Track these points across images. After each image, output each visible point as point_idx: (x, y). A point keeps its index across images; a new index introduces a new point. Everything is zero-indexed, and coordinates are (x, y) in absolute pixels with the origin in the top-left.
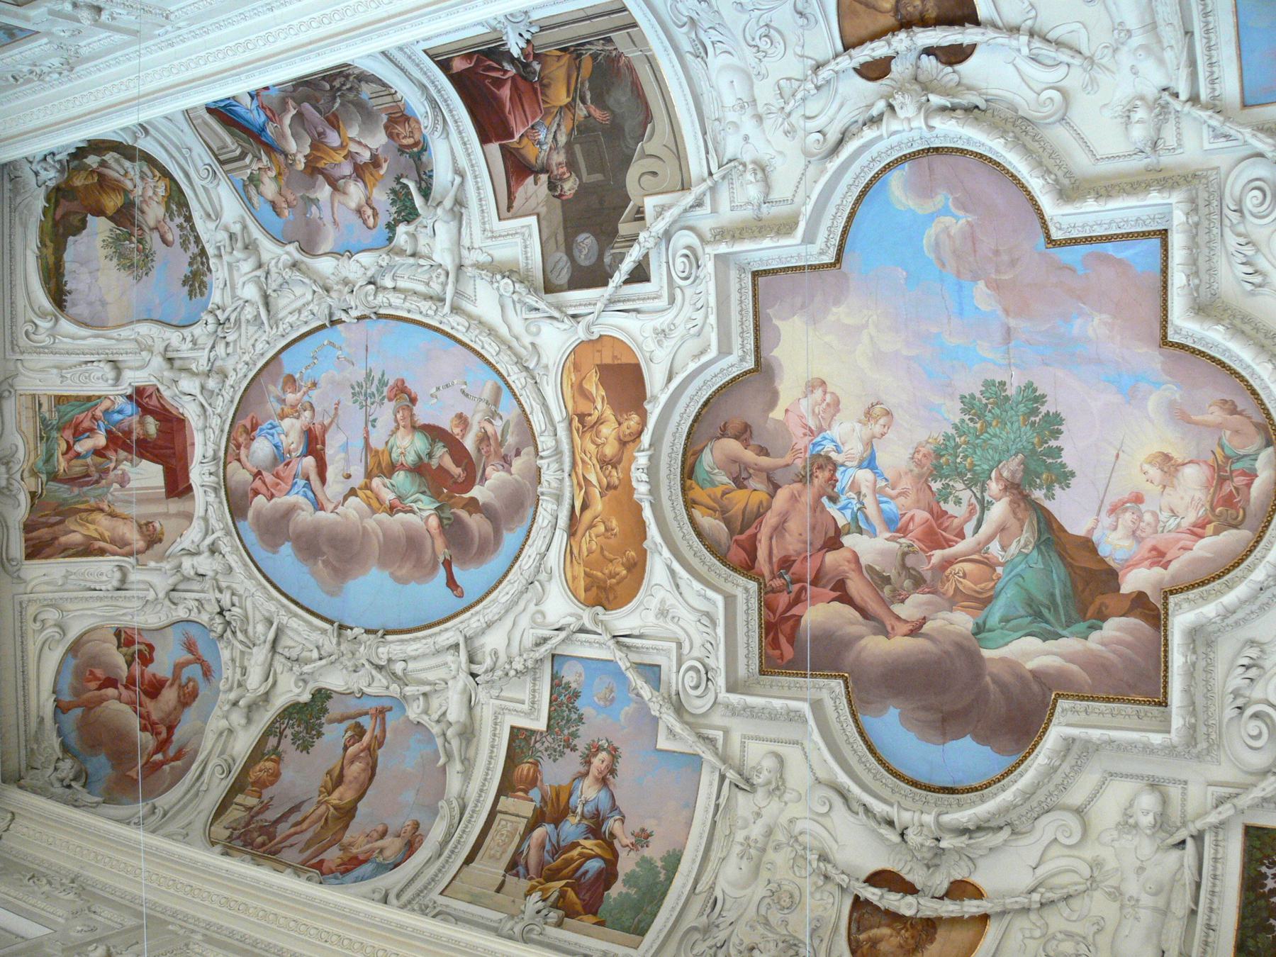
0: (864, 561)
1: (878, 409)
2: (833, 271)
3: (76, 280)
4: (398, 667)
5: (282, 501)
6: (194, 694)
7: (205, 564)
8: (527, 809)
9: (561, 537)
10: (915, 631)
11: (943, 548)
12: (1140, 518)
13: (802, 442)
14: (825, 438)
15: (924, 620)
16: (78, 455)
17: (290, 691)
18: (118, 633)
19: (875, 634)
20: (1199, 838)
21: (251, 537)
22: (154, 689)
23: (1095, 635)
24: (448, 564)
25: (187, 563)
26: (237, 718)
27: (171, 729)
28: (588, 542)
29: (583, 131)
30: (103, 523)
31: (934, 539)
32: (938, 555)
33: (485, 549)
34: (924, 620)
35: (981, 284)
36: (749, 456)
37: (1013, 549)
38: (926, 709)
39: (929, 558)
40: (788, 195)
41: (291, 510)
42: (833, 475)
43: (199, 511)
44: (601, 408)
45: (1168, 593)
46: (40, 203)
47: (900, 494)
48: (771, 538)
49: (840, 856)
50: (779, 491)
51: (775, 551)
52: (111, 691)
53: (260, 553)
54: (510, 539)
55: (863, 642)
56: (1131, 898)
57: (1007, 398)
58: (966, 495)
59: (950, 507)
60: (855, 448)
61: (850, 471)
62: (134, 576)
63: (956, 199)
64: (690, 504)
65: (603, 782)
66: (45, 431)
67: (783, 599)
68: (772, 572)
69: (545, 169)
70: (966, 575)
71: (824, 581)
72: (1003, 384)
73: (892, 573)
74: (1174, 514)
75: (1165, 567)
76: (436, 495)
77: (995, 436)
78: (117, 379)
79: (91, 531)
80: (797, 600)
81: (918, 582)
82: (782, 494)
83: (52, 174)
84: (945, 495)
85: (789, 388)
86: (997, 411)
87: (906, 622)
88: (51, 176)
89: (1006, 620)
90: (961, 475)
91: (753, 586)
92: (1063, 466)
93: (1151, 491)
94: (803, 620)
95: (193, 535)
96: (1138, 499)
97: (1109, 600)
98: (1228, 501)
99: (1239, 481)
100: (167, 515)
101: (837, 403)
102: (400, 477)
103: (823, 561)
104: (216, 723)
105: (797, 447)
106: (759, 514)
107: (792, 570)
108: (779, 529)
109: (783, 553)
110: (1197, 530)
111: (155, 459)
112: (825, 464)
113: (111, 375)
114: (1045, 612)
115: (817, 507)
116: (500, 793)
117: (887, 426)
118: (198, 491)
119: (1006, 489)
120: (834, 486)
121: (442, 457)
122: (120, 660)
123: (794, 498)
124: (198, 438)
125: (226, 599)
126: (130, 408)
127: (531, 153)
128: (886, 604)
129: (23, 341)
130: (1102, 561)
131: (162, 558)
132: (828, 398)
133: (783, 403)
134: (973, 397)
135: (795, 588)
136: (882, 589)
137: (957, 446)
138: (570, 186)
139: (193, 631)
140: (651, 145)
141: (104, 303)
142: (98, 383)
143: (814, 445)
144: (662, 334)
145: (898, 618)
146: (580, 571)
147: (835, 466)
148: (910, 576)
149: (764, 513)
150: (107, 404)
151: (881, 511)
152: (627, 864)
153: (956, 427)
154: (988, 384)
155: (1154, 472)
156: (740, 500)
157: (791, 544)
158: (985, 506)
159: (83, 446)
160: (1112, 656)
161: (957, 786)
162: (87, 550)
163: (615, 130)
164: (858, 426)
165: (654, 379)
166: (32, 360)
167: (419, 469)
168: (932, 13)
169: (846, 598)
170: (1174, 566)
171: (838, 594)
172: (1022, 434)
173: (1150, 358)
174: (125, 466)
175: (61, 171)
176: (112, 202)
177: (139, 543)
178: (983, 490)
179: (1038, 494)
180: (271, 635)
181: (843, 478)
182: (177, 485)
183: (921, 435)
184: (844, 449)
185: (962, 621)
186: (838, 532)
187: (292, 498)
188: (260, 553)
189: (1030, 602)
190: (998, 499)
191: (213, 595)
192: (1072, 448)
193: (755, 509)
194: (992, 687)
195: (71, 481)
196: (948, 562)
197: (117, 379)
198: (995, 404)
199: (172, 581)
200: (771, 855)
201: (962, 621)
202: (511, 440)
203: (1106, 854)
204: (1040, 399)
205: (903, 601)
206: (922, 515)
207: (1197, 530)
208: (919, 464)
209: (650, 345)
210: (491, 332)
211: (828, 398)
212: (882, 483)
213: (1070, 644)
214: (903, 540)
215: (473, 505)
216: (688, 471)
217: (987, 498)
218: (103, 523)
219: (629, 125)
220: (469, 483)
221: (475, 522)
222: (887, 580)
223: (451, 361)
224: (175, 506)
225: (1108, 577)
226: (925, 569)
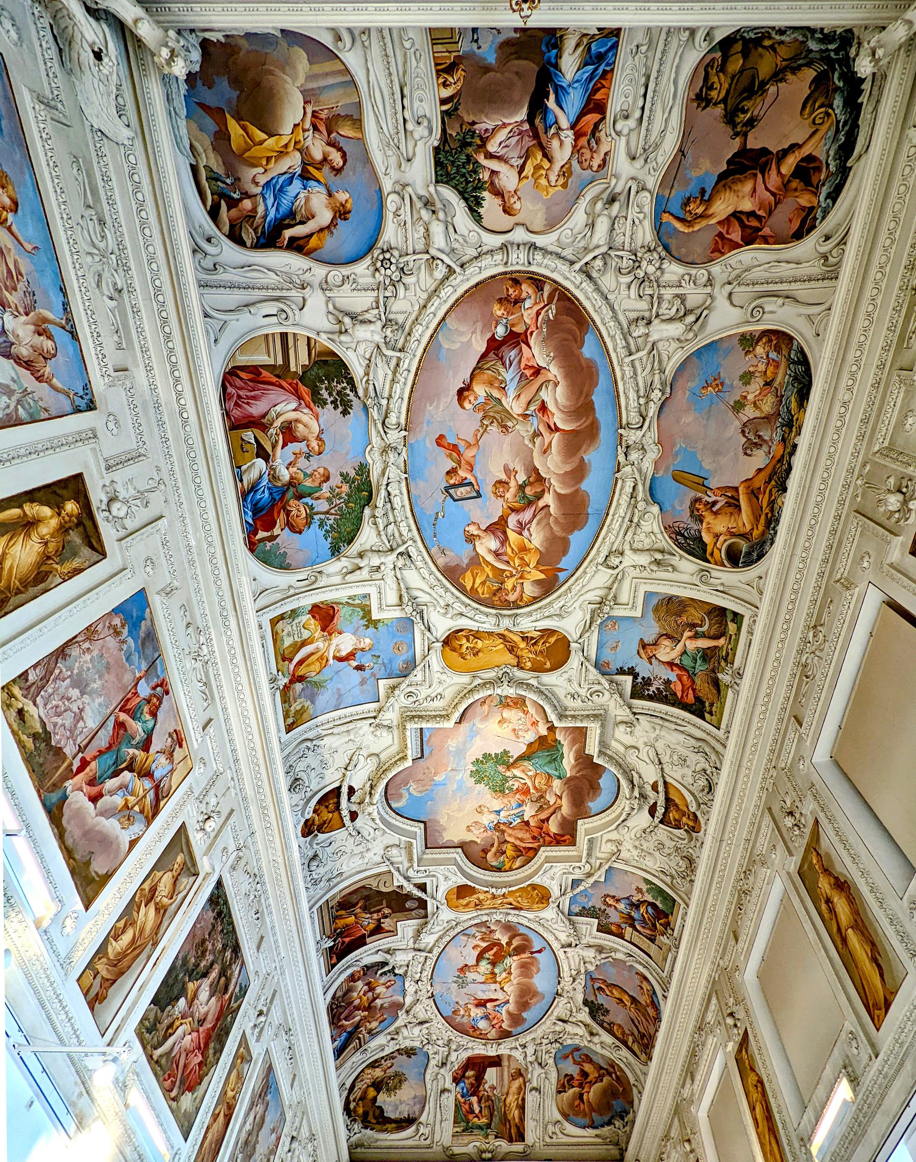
3: (404, 1111)
4: (574, 973)
5: (504, 1016)
6: (587, 1056)
7: (530, 1050)
8: (629, 930)
9: (522, 913)
10: (560, 798)
16: (481, 1111)
17: (584, 1015)
18: (559, 1092)
20: (635, 714)
21: (519, 1029)
22: (584, 1074)
24: (532, 953)
25: (529, 1059)
26: (596, 1039)
27: (601, 1068)
28: (525, 903)
29: (365, 909)
30: (511, 1099)
31: (526, 792)
33: (526, 939)
36: (494, 850)
41: (508, 1012)
43: (507, 1052)
44: (473, 899)
46: (368, 1132)
49: (645, 825)
52: (585, 1097)
53: (526, 1026)
54: (522, 930)
59: (515, 788)
60: (493, 817)
62: (535, 1084)
64: (511, 870)
65: (618, 901)
66: (469, 1129)
67: (547, 838)
69: (379, 920)
70: (540, 782)
76: (505, 957)
78: (449, 1091)
79: (514, 1105)
80: (548, 835)
81: (542, 797)
82: (508, 839)
83: (356, 1126)
84: (511, 789)
85: (468, 837)
88: (357, 1127)
91: (542, 849)
93: (511, 726)
95: (518, 1054)
96: (514, 730)
97: (549, 739)
98: (516, 704)
100: (509, 1067)
102: (497, 970)
104: (598, 1049)
106: (516, 846)
108: (521, 840)
110: (526, 713)
111: (484, 1072)
113: (446, 1094)
116: (623, 938)
118: (499, 1053)
121: (489, 955)
122: (571, 1091)
123: (510, 835)
124: (476, 1052)
125: (545, 1041)
126: (462, 1085)
127: (372, 926)
128: (550, 807)
129: (428, 1142)
131: (527, 1069)
138: (387, 911)
139: (558, 1056)
140: (374, 884)
141: (415, 1097)
142: (449, 1101)
144: (446, 878)
146: (535, 906)
150: (459, 1096)
152: (649, 898)
155: (505, 725)
156: (510, 852)
158: (515, 777)
159: (477, 1109)
162: (522, 1108)
163: (367, 898)
165: (463, 881)
166: (437, 1137)
167: (494, 964)
169: (548, 819)
172: (489, 766)
174: (487, 1086)
175: (355, 1120)
176: (372, 1093)
177: (521, 1079)
179: (511, 760)
180: (560, 1023)
181: (503, 820)
182: (496, 1062)
183: (489, 796)
185: (557, 784)
187: (504, 1012)
188: (526, 1026)
189: (550, 762)
191: (544, 1048)
192: (495, 750)
195: (492, 1115)
196: (535, 788)
197: (449, 1091)
199: (536, 1065)
200: (644, 847)
202: (484, 930)
203: (642, 740)
204: (477, 760)
206: (518, 796)
207: (526, 713)
209: (450, 883)
210: (441, 938)
213: (565, 750)
215: (509, 944)
216: (499, 870)
218: (511, 1099)
219: (366, 893)
220: (500, 945)
221: (516, 943)
223: (452, 951)
224: (505, 1063)
225: (542, 739)
226: (537, 795)
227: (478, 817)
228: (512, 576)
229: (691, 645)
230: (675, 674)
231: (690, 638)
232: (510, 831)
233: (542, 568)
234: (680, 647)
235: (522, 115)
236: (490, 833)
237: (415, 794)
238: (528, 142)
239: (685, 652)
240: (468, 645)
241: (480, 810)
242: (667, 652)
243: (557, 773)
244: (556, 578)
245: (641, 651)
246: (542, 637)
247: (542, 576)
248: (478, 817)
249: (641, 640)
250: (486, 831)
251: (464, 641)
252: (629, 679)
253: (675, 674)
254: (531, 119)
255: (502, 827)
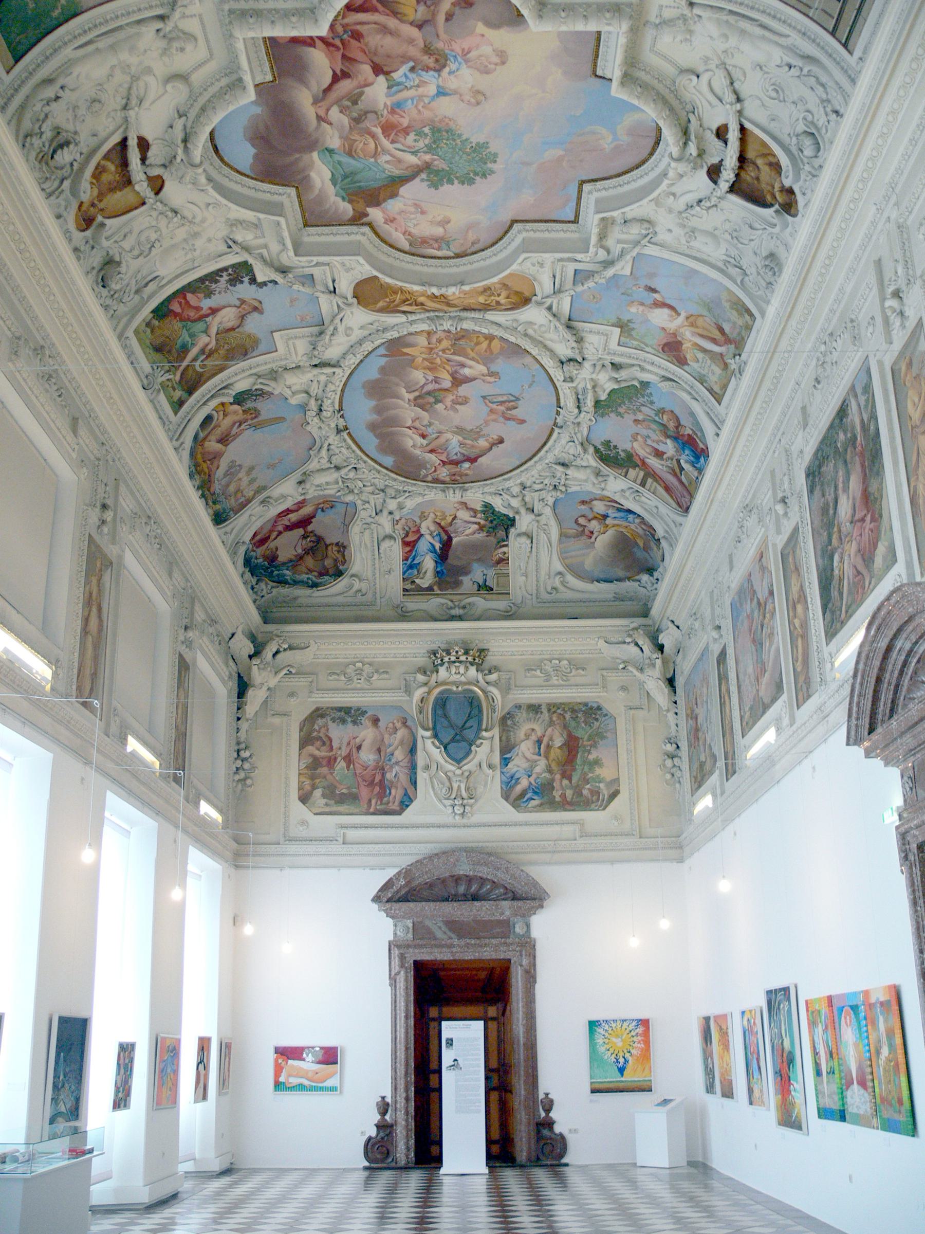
0: (366, 89)
1: (481, 98)
2: (590, 72)
10: (319, 118)
11: (383, 133)
12: (412, 214)
13: (457, 47)
14: (460, 64)
15: (331, 124)
19: (313, 96)
23: (339, 200)
31: (388, 129)
32: (378, 131)
34: (331, 124)
35: (562, 153)
37: (387, 166)
38: (267, 127)
39: (375, 126)
40: (660, 46)
42: (431, 69)
45: (370, 225)
47: (419, 111)
48: (375, 23)
50: (416, 30)
51: (366, 27)
55: (304, 89)
56: (193, 245)
57: (485, 163)
58: (421, 144)
60: (452, 83)
61: (435, 81)
63: (622, 145)
68: (347, 25)
71: (347, 64)
72: (495, 162)
73: (361, 105)
74: (415, 225)
75: (385, 223)
77: (461, 157)
81: (357, 120)
82: (414, 32)
85: (502, 37)
86: (477, 159)
87: (327, 114)
89: (339, 163)
90: (434, 142)
92: (442, 185)
93: (430, 217)
94: (312, 49)
96: (423, 213)
99: (436, 245)
101: (487, 72)
103: (362, 63)
105: (453, 43)
106: (395, 14)
107: (352, 40)
108: (385, 30)
109: (364, 33)
112: (440, 62)
114: (349, 179)
115: (405, 59)
117: (469, 102)
119: (427, 163)
120: (423, 70)
123: (411, 41)
130: (385, 200)
132: (492, 66)
133: (491, 33)
134: (488, 148)
135: (337, 42)
136: (348, 100)
137: (454, 140)
143: (455, 57)
145: (328, 110)
147: (439, 71)
148: (360, 116)
149: (398, 18)
151: (406, 100)
153: (467, 140)
154: (496, 155)
157: (374, 40)
158: (414, 153)
160: (328, 206)
161: (220, 152)
164: (469, 86)
168: (743, 174)
169: (336, 79)
170: (387, 226)
171: (338, 72)
173: (506, 216)
178: (424, 152)
181: (430, 76)
184: (452, 77)
186: (387, 73)
189: (353, 173)
190: (419, 159)
192: (453, 191)
193: (400, 11)
194: (292, 158)
196: (373, 136)
198: (482, 158)
201: (334, 142)
205: (341, 112)
206: (405, 122)
208: (441, 121)
211: (492, 66)
212: (426, 100)
213: (331, 190)
214: (386, 111)
217: (419, 154)
222: (355, 103)
226: (367, 124)
227: (483, 82)
228: (444, 351)
229: (203, 340)
230: (205, 308)
231: (207, 345)
232: (413, 51)
233: (409, 357)
234: (213, 331)
235: (455, 541)
236: (457, 47)
237: (604, 131)
238: (450, 529)
239: (206, 331)
240: (497, 299)
241: (479, 96)
242: (227, 317)
243: (336, 157)
244: (388, 349)
245: (257, 304)
246: (397, 306)
247: (405, 350)
248: (483, 82)
249: (261, 312)
250: (464, 53)
251: (503, 301)
252: (260, 278)
253: (205, 308)
254: (450, 539)
255: (430, 61)
